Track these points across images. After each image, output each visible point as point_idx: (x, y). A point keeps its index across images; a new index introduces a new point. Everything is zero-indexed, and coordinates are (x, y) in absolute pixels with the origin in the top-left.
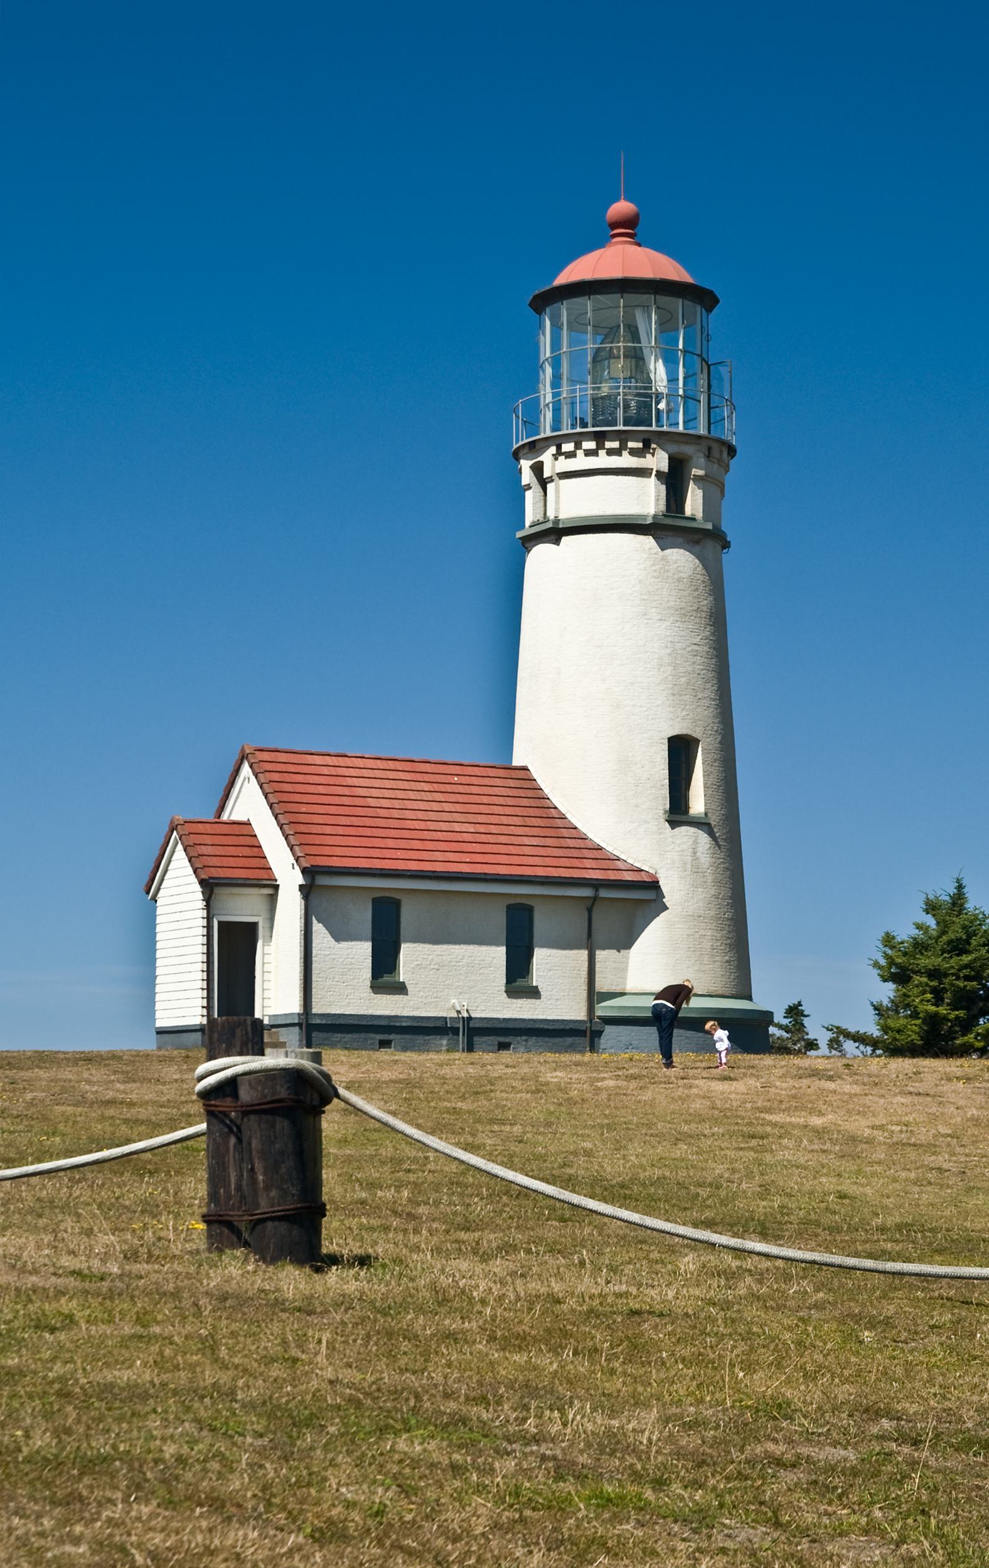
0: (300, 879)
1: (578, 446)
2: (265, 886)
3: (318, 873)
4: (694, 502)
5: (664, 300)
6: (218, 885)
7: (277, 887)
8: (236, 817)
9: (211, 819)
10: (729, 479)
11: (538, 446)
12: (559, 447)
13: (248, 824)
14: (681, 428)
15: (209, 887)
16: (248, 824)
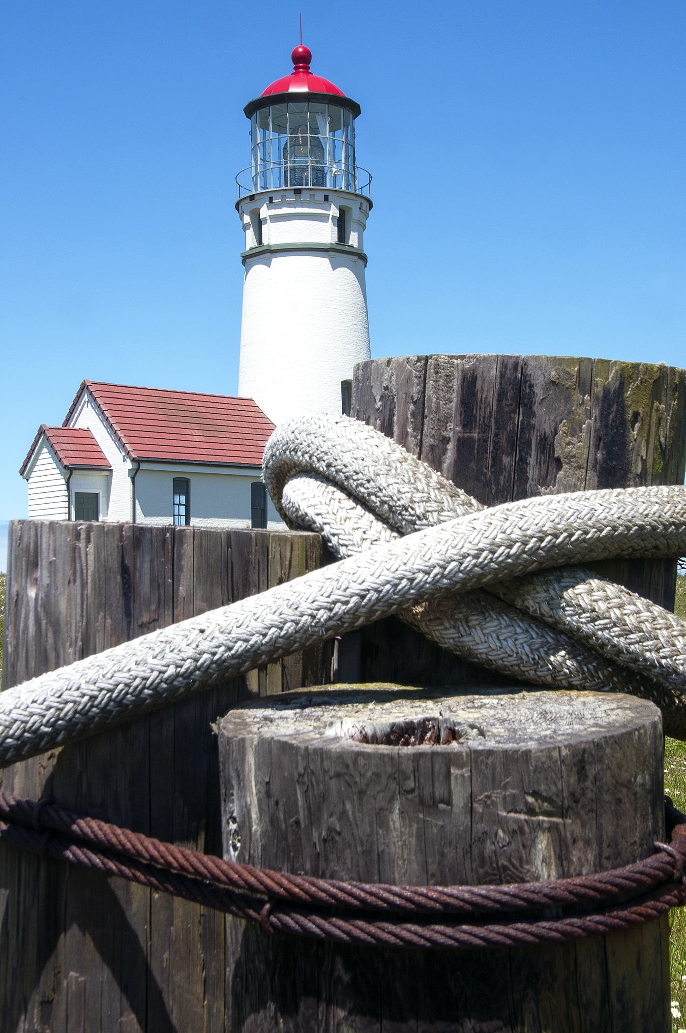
0: (129, 465)
1: (283, 197)
2: (104, 470)
3: (142, 461)
4: (353, 239)
5: (333, 108)
6: (75, 469)
7: (111, 471)
8: (77, 427)
9: (60, 426)
10: (368, 223)
11: (256, 198)
12: (271, 199)
13: (88, 430)
14: (343, 188)
15: (69, 471)
16: (88, 430)
